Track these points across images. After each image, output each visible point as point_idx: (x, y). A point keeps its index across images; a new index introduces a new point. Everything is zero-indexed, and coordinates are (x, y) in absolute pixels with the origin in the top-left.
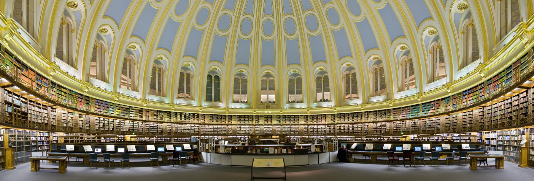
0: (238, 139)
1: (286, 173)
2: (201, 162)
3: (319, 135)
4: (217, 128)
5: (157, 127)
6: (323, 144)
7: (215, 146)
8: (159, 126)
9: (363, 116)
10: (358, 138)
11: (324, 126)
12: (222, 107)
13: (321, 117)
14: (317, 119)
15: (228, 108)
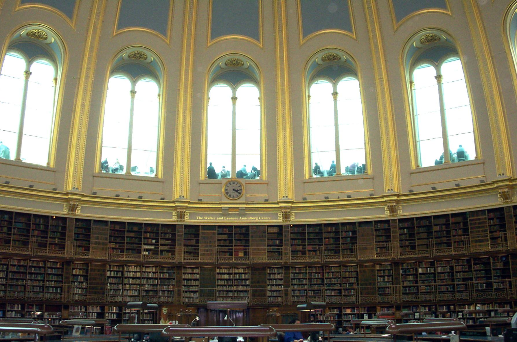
4: (22, 270)
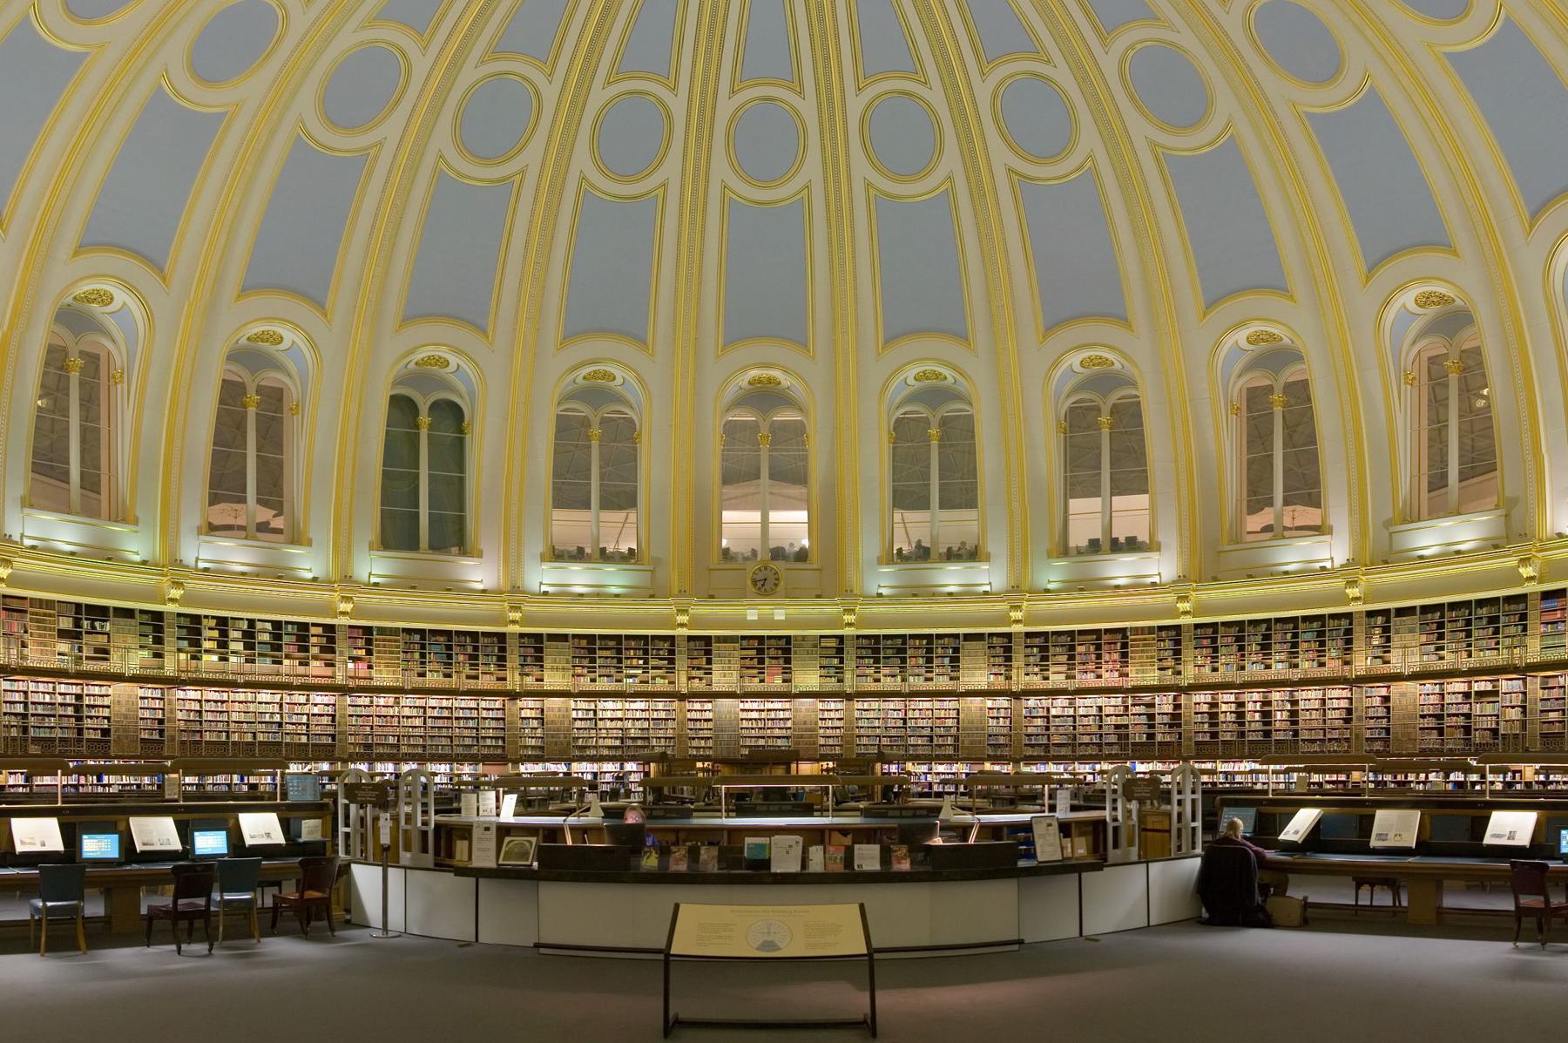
0: (579, 781)
1: (878, 994)
2: (348, 924)
3: (1083, 759)
4: (446, 713)
5: (78, 708)
6: (1107, 814)
7: (438, 826)
8: (87, 701)
9: (1355, 636)
10: (1327, 778)
11: (1113, 701)
12: (480, 586)
13: (1098, 647)
14: (1072, 658)
15: (515, 589)
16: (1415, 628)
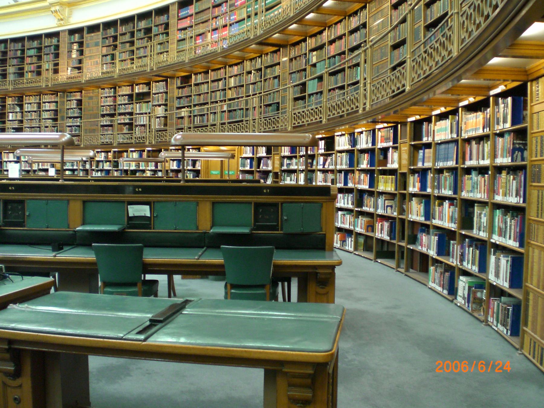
16: (99, 42)
